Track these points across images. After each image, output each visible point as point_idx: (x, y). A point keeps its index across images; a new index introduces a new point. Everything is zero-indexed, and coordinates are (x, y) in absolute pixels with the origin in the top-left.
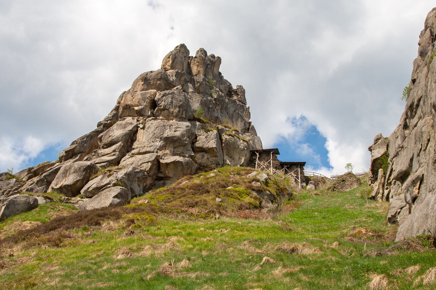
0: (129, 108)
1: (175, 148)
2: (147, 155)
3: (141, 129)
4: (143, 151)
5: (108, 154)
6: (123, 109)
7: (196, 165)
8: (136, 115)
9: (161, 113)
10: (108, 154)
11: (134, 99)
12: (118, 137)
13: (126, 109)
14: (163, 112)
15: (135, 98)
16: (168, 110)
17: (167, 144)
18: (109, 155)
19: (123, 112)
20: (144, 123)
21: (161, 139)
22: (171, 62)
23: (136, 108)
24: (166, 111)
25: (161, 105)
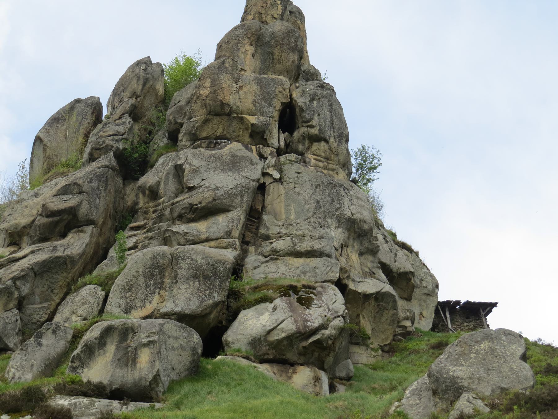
0: (229, 115)
1: (361, 254)
2: (314, 262)
3: (276, 180)
4: (305, 246)
5: (208, 240)
6: (209, 113)
7: (402, 315)
8: (247, 139)
9: (308, 148)
10: (208, 240)
11: (241, 92)
12: (231, 195)
13: (217, 114)
14: (315, 146)
15: (245, 89)
16: (327, 141)
17: (348, 238)
18: (213, 243)
19: (206, 121)
20: (279, 167)
21: (339, 220)
22: (280, 7)
23: (252, 120)
24: (323, 143)
25: (313, 123)
